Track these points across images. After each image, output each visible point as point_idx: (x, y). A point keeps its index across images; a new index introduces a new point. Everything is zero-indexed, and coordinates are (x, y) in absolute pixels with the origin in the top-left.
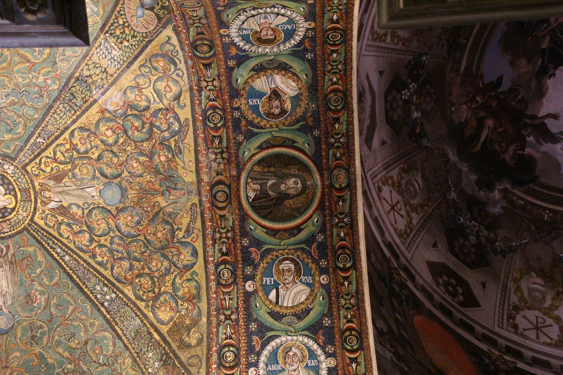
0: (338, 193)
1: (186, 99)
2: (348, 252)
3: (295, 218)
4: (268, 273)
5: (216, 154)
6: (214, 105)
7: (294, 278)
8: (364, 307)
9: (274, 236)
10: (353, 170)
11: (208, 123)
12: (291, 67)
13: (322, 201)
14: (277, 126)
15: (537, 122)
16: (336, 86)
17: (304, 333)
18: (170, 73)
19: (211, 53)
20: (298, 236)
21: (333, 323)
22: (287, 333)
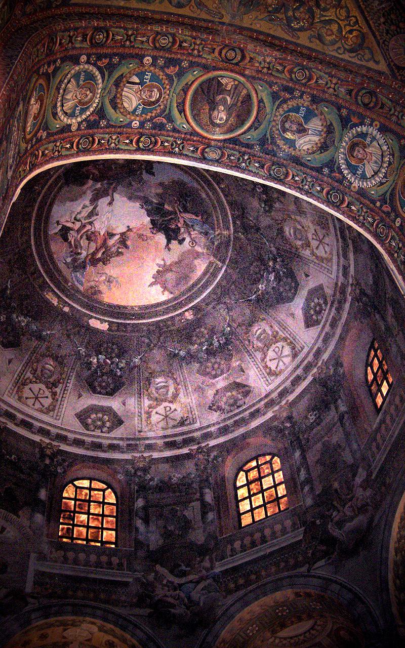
0: (201, 149)
1: (316, 45)
2: (151, 147)
3: (192, 110)
4: (154, 78)
5: (269, 63)
6: (313, 79)
7: (144, 99)
8: (106, 153)
9: (183, 90)
10: (216, 165)
11: (298, 68)
12: (321, 153)
13: (198, 135)
14: (274, 120)
15: (110, 192)
16: (291, 177)
17: (100, 103)
18: (343, 41)
19: (360, 103)
20: (176, 109)
21: (101, 128)
22: (104, 89)
